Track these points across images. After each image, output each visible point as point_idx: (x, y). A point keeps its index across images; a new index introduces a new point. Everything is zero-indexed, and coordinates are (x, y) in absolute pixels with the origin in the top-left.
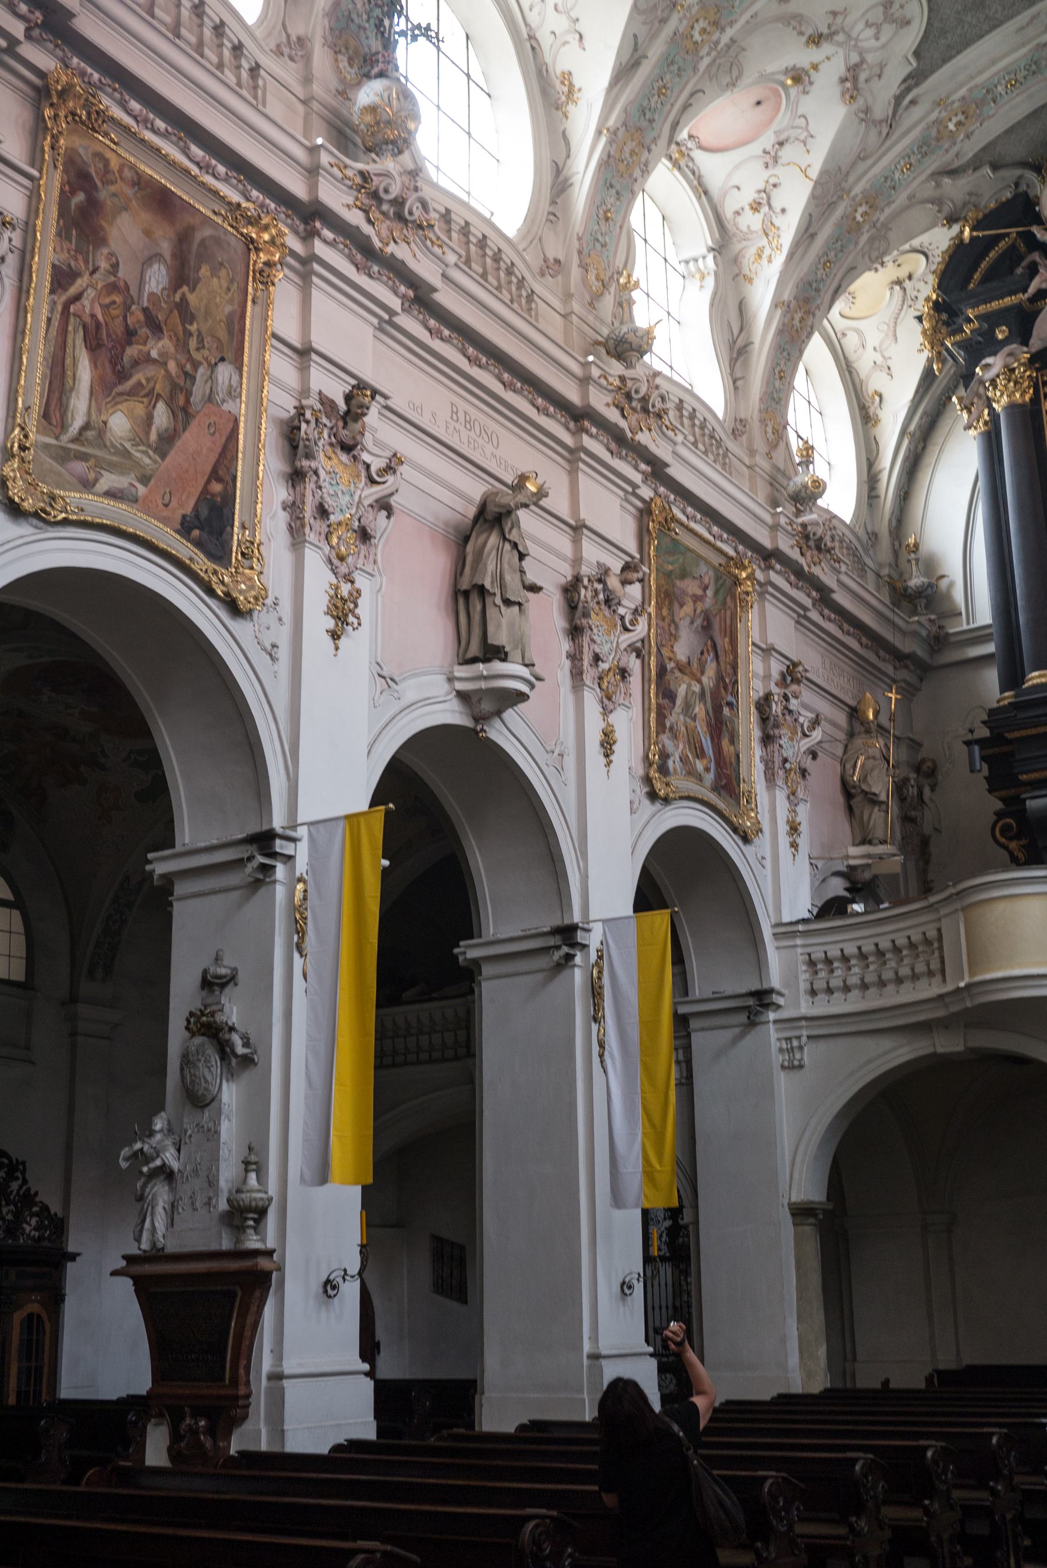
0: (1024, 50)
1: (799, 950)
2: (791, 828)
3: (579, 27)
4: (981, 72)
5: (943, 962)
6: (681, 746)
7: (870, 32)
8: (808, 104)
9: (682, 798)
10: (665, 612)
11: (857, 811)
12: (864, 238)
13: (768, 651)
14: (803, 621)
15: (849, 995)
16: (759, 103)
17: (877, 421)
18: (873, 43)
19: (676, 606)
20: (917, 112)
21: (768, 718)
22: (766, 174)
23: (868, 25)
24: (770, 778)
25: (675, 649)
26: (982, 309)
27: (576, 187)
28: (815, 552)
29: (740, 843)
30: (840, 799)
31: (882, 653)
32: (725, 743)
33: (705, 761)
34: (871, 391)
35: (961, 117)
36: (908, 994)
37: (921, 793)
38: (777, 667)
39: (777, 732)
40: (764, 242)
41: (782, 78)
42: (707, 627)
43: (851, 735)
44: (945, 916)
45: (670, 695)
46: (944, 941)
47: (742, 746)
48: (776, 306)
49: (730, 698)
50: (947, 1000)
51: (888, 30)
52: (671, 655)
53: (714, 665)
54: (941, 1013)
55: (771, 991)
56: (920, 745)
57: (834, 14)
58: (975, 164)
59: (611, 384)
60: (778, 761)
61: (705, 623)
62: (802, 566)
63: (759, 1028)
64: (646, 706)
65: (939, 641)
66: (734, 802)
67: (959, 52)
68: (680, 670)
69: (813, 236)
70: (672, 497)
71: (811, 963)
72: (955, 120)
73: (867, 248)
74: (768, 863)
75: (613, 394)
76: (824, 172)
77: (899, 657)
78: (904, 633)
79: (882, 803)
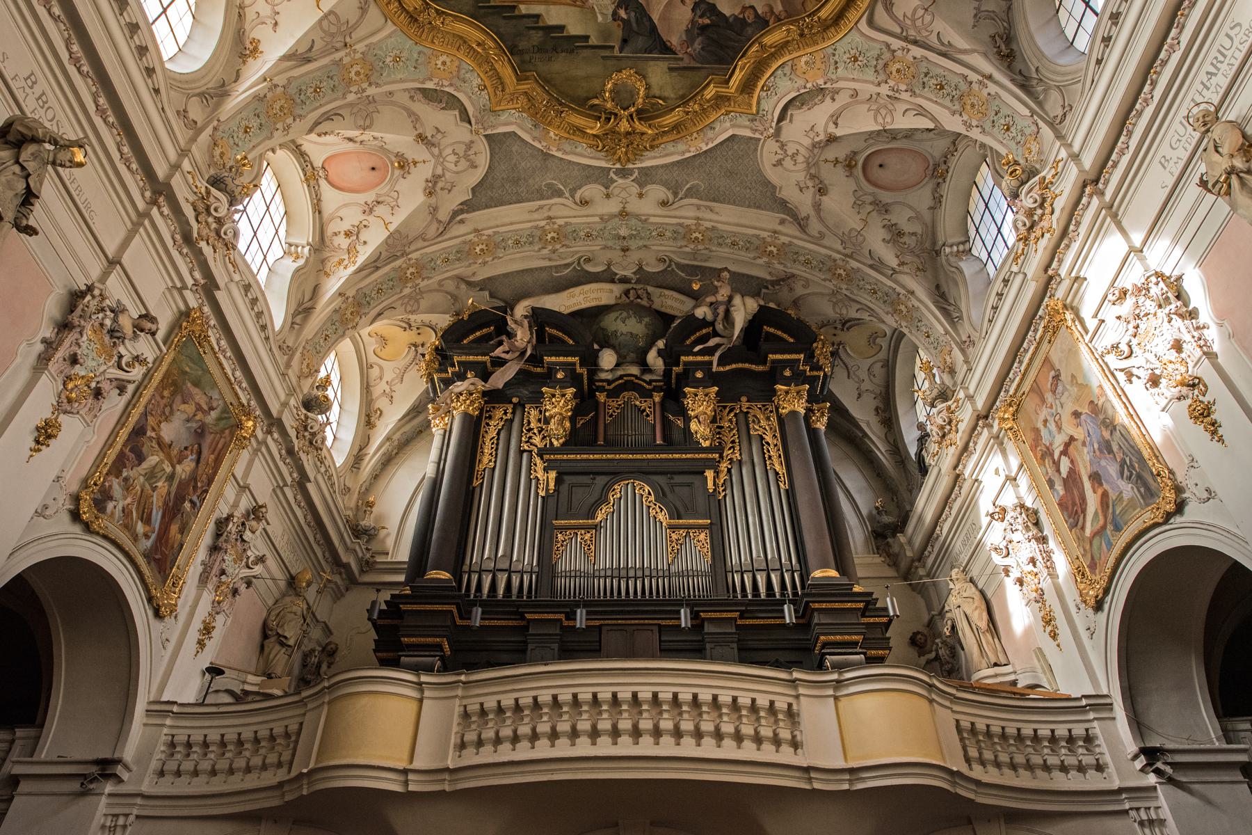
0: (530, 225)
1: (165, 731)
2: (205, 628)
3: (276, 17)
4: (502, 226)
5: (293, 755)
6: (129, 500)
7: (452, 158)
8: (402, 185)
9: (105, 537)
10: (166, 393)
11: (266, 650)
12: (407, 291)
13: (244, 488)
14: (279, 492)
15: (196, 779)
16: (373, 169)
17: (374, 426)
18: (451, 166)
19: (178, 399)
20: (462, 229)
21: (221, 535)
22: (362, 217)
23: (455, 153)
24: (203, 579)
25: (163, 425)
26: (463, 358)
27: (231, 98)
28: (307, 443)
29: (150, 613)
30: (257, 636)
31: (327, 554)
32: (174, 528)
33: (147, 528)
34: (376, 406)
35: (484, 247)
36: (252, 781)
37: (319, 666)
38: (245, 503)
39: (224, 545)
40: (346, 257)
41: (394, 159)
42: (200, 433)
43: (284, 595)
44: (310, 710)
45: (141, 458)
46: (302, 735)
47: (189, 539)
48: (340, 294)
49: (195, 498)
50: (286, 788)
51: (463, 164)
52: (156, 427)
53: (193, 465)
54: (275, 803)
55: (118, 761)
56: (331, 633)
57: (438, 130)
58: (483, 285)
59: (196, 187)
60: (215, 570)
61: (199, 431)
62: (294, 446)
63: (89, 799)
64: (109, 442)
65: (368, 565)
66: (160, 579)
67: (496, 206)
68: (159, 444)
69: (377, 268)
70: (212, 322)
71: (172, 745)
72: (481, 247)
73: (406, 300)
74: (171, 647)
75: (196, 198)
76: (397, 231)
77: (336, 562)
78: (347, 549)
79: (289, 646)
